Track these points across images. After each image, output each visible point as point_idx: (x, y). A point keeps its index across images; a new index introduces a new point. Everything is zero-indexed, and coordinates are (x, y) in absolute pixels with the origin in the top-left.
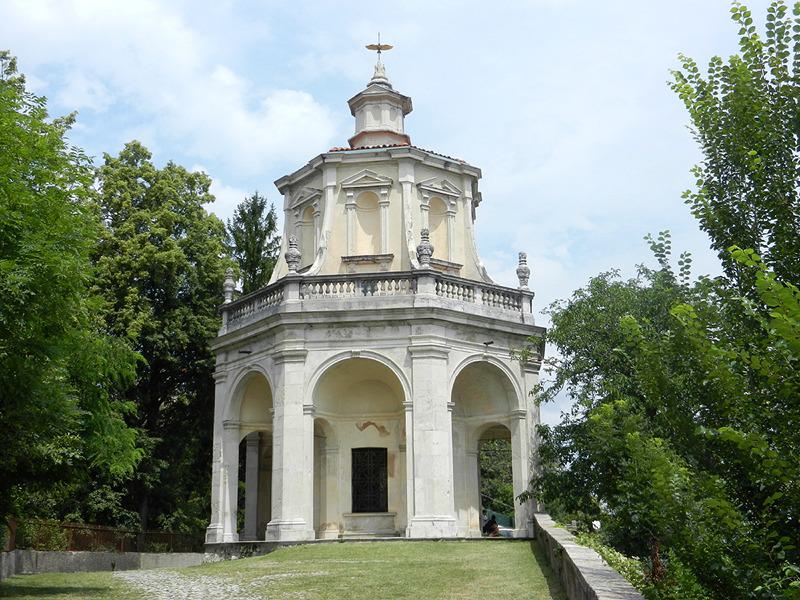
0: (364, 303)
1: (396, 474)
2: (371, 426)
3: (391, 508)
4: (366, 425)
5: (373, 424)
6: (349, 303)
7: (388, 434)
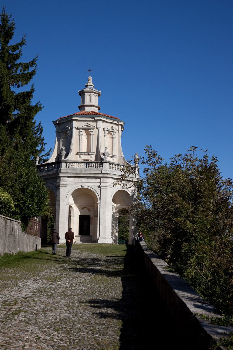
0: (86, 170)
1: (93, 223)
2: (85, 208)
3: (91, 234)
4: (84, 208)
5: (86, 208)
6: (81, 170)
7: (91, 211)
